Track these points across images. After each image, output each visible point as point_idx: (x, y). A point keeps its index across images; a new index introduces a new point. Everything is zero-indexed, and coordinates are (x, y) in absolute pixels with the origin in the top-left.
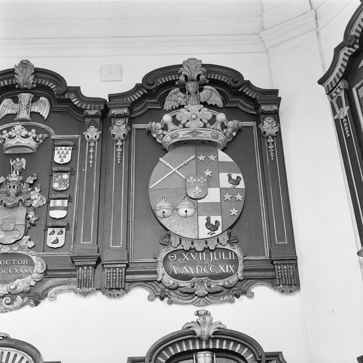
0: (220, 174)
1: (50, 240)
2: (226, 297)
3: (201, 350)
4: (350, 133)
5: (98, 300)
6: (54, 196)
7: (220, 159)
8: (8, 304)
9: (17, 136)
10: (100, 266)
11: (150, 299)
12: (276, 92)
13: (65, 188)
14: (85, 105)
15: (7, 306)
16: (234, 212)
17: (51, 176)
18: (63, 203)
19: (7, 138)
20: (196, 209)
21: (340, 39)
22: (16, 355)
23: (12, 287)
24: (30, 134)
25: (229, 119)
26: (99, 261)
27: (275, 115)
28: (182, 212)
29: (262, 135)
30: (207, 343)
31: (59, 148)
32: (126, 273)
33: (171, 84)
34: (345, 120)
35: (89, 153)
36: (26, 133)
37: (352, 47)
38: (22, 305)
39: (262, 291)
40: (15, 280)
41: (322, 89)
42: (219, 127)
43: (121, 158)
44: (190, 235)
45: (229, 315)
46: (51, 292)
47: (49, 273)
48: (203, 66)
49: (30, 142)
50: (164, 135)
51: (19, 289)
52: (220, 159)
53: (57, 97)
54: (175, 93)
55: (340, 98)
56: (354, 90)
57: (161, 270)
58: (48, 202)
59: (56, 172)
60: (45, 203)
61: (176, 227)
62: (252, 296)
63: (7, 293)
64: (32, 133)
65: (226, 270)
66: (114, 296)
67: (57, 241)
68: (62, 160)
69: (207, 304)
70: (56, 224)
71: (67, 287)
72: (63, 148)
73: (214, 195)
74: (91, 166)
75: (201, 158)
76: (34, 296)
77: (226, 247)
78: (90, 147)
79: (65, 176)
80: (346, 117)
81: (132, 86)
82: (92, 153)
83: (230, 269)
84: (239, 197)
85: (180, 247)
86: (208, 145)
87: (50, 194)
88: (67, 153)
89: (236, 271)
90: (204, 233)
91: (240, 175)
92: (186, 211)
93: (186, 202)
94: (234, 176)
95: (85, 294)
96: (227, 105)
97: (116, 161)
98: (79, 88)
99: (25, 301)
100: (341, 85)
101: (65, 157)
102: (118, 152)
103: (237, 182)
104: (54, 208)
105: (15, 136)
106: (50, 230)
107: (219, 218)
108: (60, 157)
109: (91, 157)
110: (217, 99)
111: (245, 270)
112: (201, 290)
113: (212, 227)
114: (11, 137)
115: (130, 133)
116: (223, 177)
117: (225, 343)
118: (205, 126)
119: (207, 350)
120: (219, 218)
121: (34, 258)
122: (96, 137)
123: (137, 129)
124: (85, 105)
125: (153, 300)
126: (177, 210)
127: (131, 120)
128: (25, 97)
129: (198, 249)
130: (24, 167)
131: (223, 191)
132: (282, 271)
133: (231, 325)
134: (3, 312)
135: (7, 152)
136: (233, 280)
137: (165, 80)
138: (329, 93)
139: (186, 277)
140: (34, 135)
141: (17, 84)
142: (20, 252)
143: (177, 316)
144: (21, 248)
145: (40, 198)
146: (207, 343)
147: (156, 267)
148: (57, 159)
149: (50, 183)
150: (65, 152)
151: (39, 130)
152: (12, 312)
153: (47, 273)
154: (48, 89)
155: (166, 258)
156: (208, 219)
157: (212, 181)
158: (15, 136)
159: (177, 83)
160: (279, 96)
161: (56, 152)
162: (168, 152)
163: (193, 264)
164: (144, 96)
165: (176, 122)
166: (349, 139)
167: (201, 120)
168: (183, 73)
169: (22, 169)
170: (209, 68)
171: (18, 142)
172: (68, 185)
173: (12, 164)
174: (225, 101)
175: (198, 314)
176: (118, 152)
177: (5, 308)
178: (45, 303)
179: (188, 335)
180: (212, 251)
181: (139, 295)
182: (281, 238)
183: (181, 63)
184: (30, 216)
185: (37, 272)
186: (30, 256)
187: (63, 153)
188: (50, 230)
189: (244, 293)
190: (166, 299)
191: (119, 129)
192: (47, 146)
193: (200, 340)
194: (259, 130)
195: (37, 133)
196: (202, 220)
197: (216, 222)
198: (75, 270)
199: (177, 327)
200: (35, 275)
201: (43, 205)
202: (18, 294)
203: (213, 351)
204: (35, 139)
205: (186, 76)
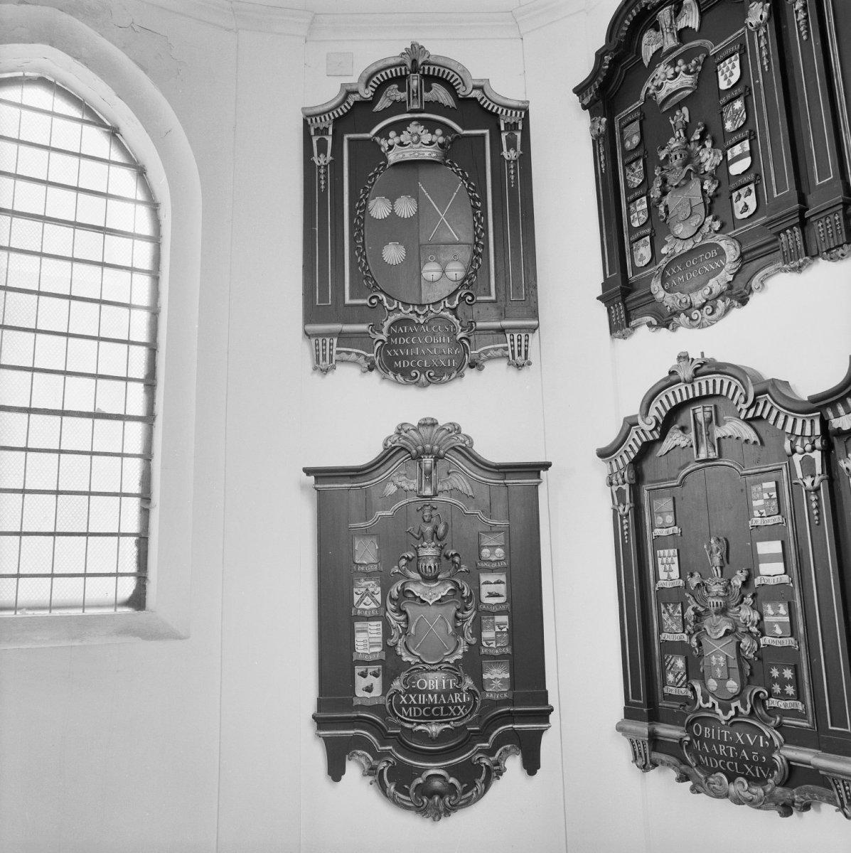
6: (730, 143)
9: (664, 82)
13: (742, 123)
15: (710, 317)
17: (722, 113)
18: (743, 148)
19: (655, 92)
22: (722, 382)
24: (677, 69)
31: (722, 65)
38: (727, 310)
40: (708, 281)
43: (808, 29)
46: (755, 283)
51: (716, 291)
58: (725, 156)
59: (726, 105)
60: (721, 158)
63: (704, 301)
64: (680, 67)
68: (729, 82)
70: (739, 183)
72: (727, 61)
74: (766, 70)
76: (739, 295)
88: (734, 67)
95: (799, 269)
97: (801, 37)
99: (728, 304)
101: (732, 74)
102: (799, 21)
105: (662, 83)
106: (735, 195)
121: (723, 244)
122: (761, 17)
130: (687, 119)
134: (708, 326)
135: (665, 109)
140: (683, 67)
141: (647, 5)
145: (712, 155)
150: (730, 66)
152: (720, 322)
158: (662, 83)
161: (720, 73)
169: (686, 122)
171: (682, 83)
172: (745, 116)
173: (672, 123)
176: (799, 21)
178: (754, 299)
185: (730, 262)
186: (718, 242)
188: (735, 195)
195: (687, 62)
198: (776, 240)
201: (720, 163)
204: (687, 72)
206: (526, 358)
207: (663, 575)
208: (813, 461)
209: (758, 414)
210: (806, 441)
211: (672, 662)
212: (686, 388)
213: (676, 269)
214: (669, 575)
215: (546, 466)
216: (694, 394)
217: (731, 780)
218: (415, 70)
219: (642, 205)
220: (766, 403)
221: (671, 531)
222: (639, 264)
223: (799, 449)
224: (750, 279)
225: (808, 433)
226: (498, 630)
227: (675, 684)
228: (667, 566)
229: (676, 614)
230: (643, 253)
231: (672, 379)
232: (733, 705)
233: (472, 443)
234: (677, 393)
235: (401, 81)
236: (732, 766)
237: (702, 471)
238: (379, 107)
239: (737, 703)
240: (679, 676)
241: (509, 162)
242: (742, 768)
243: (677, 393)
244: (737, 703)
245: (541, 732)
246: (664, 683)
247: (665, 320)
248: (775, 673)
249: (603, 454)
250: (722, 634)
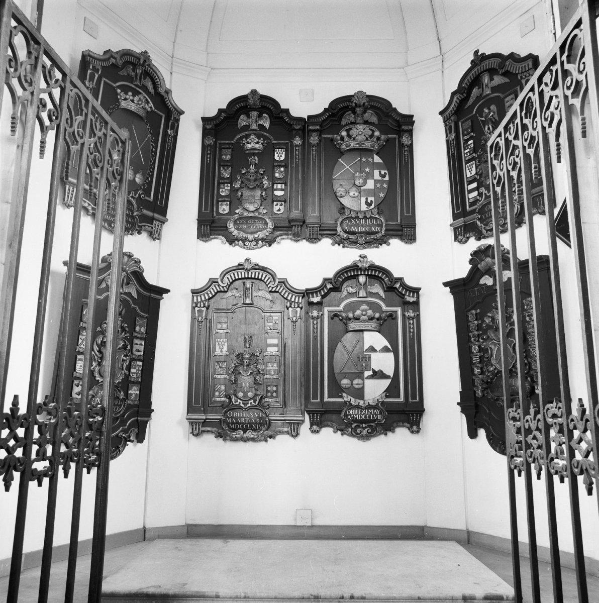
0: (375, 171)
1: (276, 208)
2: (375, 245)
3: (361, 275)
4: (454, 151)
5: (304, 245)
7: (375, 161)
8: (255, 245)
10: (304, 225)
11: (333, 244)
12: (412, 116)
14: (292, 122)
15: (254, 247)
16: (382, 195)
17: (274, 168)
20: (360, 193)
21: (455, 88)
23: (256, 236)
25: (382, 133)
26: (304, 222)
27: (410, 132)
28: (352, 194)
29: (402, 145)
30: (364, 271)
31: (277, 150)
32: (320, 230)
33: (346, 109)
34: (452, 142)
35: (296, 154)
36: (258, 140)
37: (462, 94)
38: (262, 246)
39: (395, 242)
40: (257, 232)
41: (440, 118)
42: (375, 140)
44: (356, 209)
45: (378, 256)
46: (278, 239)
47: (276, 229)
48: (368, 96)
49: (259, 146)
50: (342, 144)
52: (375, 161)
53: (275, 116)
54: (348, 114)
55: (451, 126)
56: (460, 123)
57: (339, 229)
58: (273, 185)
59: (277, 166)
61: (346, 201)
62: (389, 244)
65: (375, 230)
66: (313, 243)
67: (279, 210)
68: (280, 159)
69: (364, 248)
71: (287, 237)
72: (280, 150)
73: (370, 185)
75: (364, 160)
76: (269, 241)
77: (377, 216)
78: (296, 150)
79: (282, 169)
80: (453, 140)
81: (322, 110)
82: (297, 152)
83: (377, 229)
84: (385, 186)
85: (350, 216)
86: (368, 152)
87: (274, 180)
89: (381, 230)
90: (364, 207)
91: (387, 172)
92: (354, 194)
93: (354, 189)
94: (383, 172)
95: (297, 241)
96: (381, 123)
98: (288, 109)
100: (452, 118)
103: (384, 176)
104: (277, 190)
106: (275, 203)
107: (373, 199)
108: (278, 156)
109: (297, 157)
110: (374, 119)
111: (386, 230)
112: (361, 241)
113: (368, 204)
114: (248, 143)
115: (320, 141)
116: (376, 172)
117: (374, 272)
118: (367, 139)
119: (364, 274)
120: (373, 199)
121: (267, 220)
123: (325, 138)
124: (292, 122)
125: (334, 245)
126: (349, 193)
127: (320, 132)
128: (254, 114)
129: (360, 217)
130: (257, 162)
131: (376, 182)
132: (406, 231)
133: (378, 263)
136: (380, 235)
137: (343, 105)
138: (445, 121)
139: (353, 233)
140: (262, 142)
142: (259, 216)
143: (348, 256)
144: (260, 214)
146: (364, 271)
147: (336, 227)
148: (277, 158)
149: (274, 173)
150: (281, 152)
151: (265, 138)
153: (276, 228)
154: (269, 109)
155: (342, 222)
156: (367, 199)
157: (370, 175)
159: (350, 107)
160: (414, 120)
161: (276, 153)
162: (343, 155)
163: (357, 225)
164: (329, 116)
165: (349, 136)
166: (453, 155)
167: (365, 136)
168: (354, 101)
170: (371, 98)
174: (379, 120)
175: (360, 256)
177: (253, 248)
178: (274, 245)
179: (354, 267)
180: (368, 218)
181: (326, 242)
182: (408, 212)
183: (353, 94)
184: (263, 194)
187: (280, 153)
188: (275, 203)
189: (385, 243)
190: (342, 245)
191: (314, 139)
192: (269, 150)
193: (361, 269)
194: (400, 141)
195: (264, 140)
196: (363, 200)
197: (371, 201)
198: (291, 228)
199: (349, 263)
200: (269, 230)
202: (260, 240)
203: (368, 275)
204: (262, 144)
205: (356, 103)
206: (159, 236)
207: (218, 350)
208: (297, 311)
209: (277, 290)
210: (296, 304)
211: (219, 387)
212: (245, 273)
213: (243, 222)
214: (221, 350)
215: (167, 291)
216: (248, 276)
217: (245, 432)
218: (143, 65)
219: (228, 187)
220: (281, 287)
221: (225, 331)
222: (221, 212)
223: (293, 306)
224: (278, 236)
225: (297, 301)
226: (137, 369)
227: (219, 396)
228: (221, 346)
229: (223, 366)
230: (224, 208)
231: (240, 267)
232: (249, 402)
233: (143, 271)
234: (240, 274)
235: (135, 66)
236: (246, 426)
237: (244, 308)
238: (121, 73)
239: (252, 401)
240: (222, 393)
241: (169, 135)
242: (251, 426)
243: (240, 274)
244: (252, 401)
245: (147, 421)
246: (214, 396)
247: (232, 241)
248: (269, 389)
249: (194, 292)
250: (249, 374)
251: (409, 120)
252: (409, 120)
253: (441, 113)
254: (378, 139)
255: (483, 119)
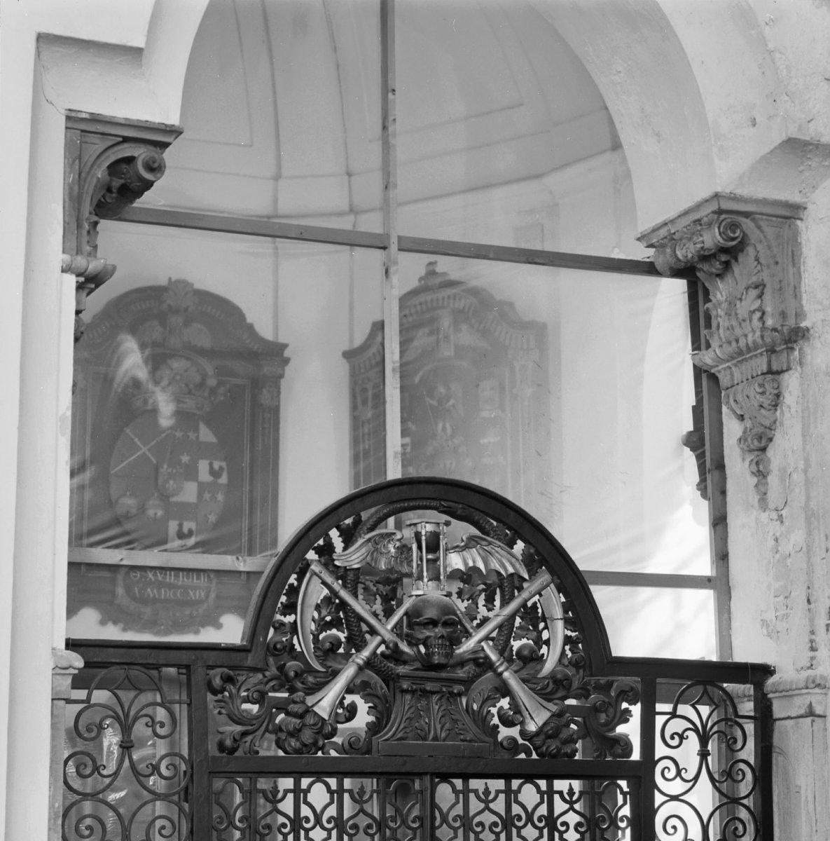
42: (206, 394)
50: (134, 396)
65: (195, 596)
83: (195, 594)
91: (224, 464)
94: (216, 465)
111: (218, 597)
131: (202, 488)
156: (181, 525)
194: (254, 398)
205: (170, 306)
251: (275, 354)
252: (275, 354)
253: (348, 355)
254: (213, 391)
255: (435, 403)
